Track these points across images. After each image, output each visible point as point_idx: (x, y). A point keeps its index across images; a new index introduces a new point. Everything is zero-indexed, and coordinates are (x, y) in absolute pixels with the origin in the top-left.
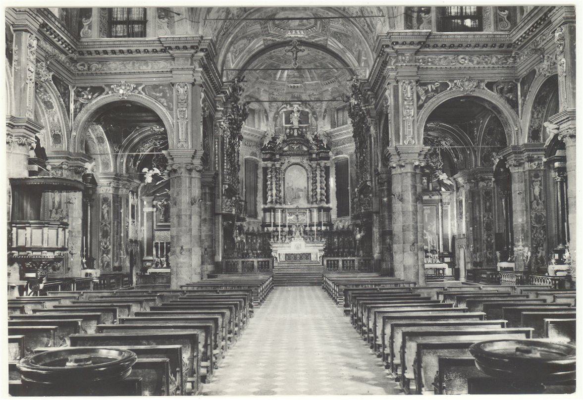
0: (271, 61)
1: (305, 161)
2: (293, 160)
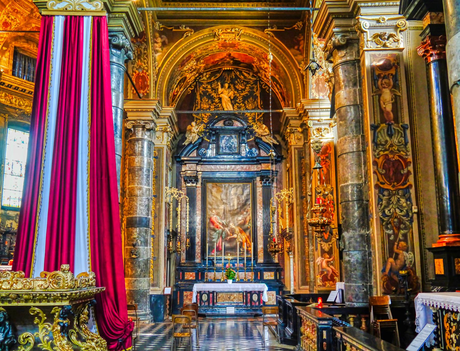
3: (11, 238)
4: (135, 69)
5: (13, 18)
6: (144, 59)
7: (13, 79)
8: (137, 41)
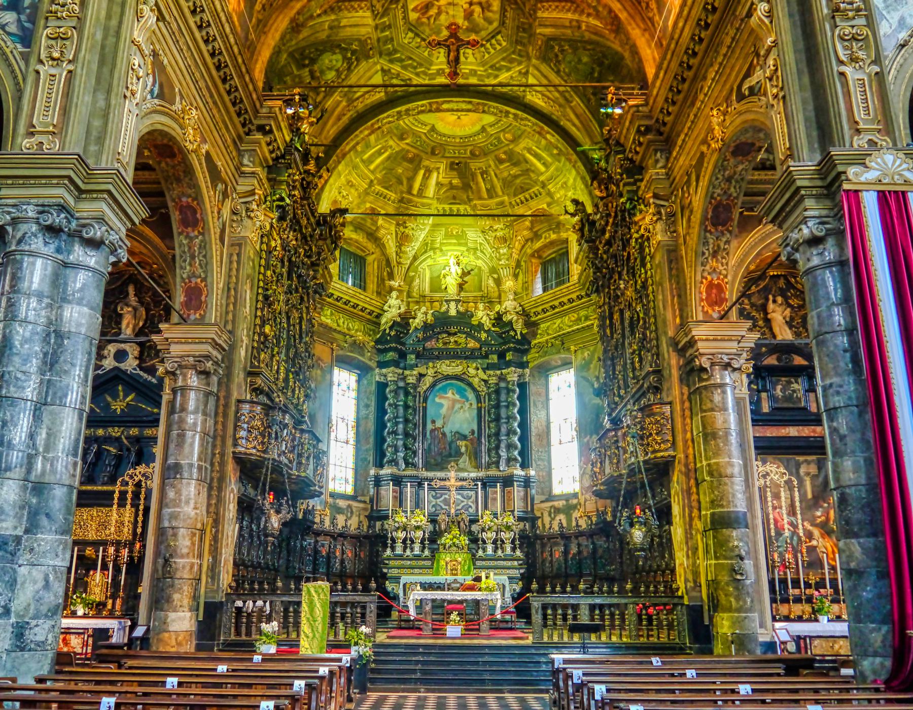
0: (403, 145)
1: (472, 371)
2: (447, 367)
3: (343, 544)
4: (706, 274)
6: (723, 258)
8: (716, 230)
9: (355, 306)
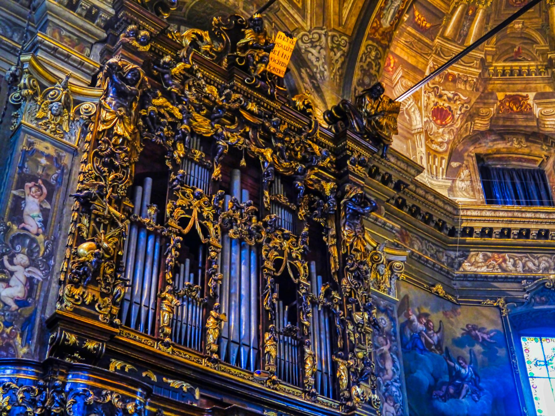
5: (451, 96)
7: (488, 214)
9: (524, 234)
